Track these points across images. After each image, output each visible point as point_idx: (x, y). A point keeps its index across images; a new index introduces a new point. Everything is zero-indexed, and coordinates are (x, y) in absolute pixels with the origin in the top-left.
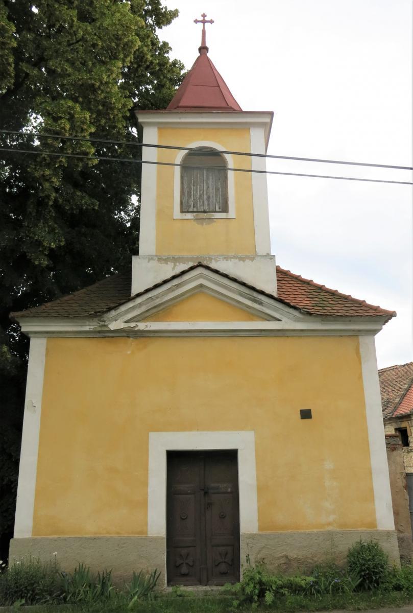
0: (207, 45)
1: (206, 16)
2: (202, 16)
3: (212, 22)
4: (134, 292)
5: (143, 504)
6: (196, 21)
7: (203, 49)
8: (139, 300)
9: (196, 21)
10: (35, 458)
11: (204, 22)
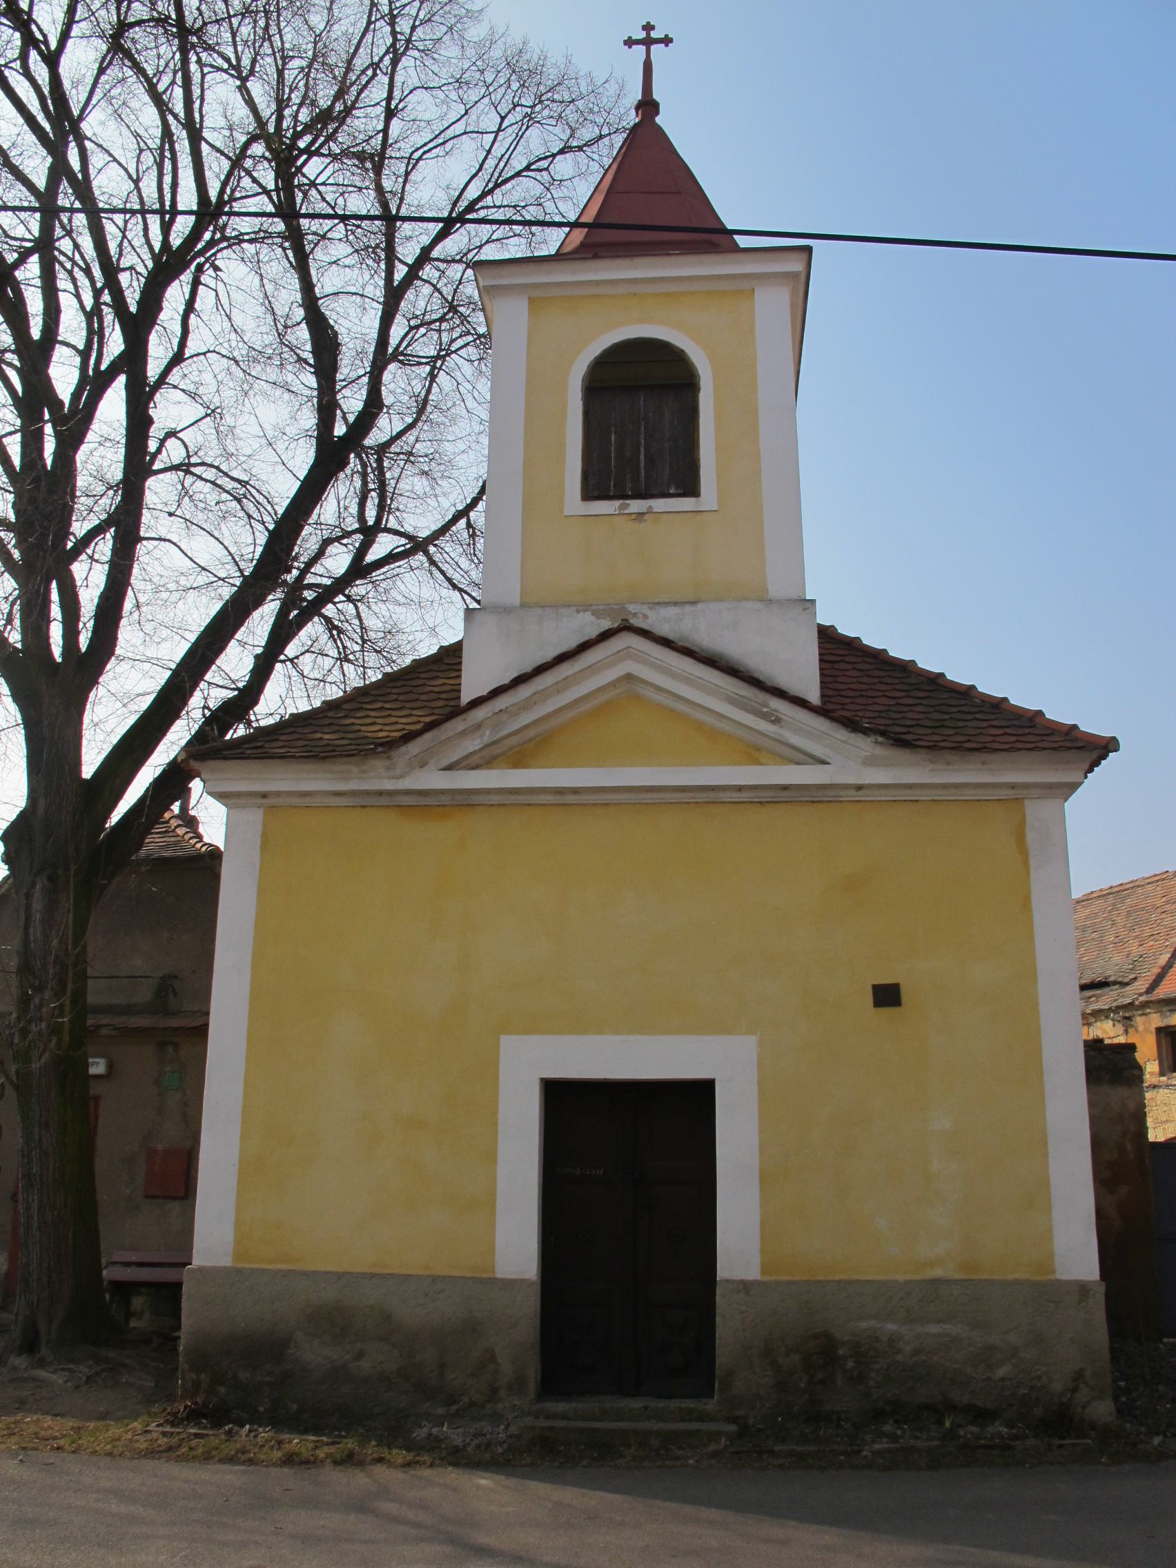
0: (656, 96)
1: (653, 28)
2: (644, 28)
3: (667, 41)
4: (465, 698)
5: (486, 1204)
6: (630, 43)
7: (648, 106)
8: (480, 714)
9: (630, 43)
10: (237, 1089)
11: (648, 42)
